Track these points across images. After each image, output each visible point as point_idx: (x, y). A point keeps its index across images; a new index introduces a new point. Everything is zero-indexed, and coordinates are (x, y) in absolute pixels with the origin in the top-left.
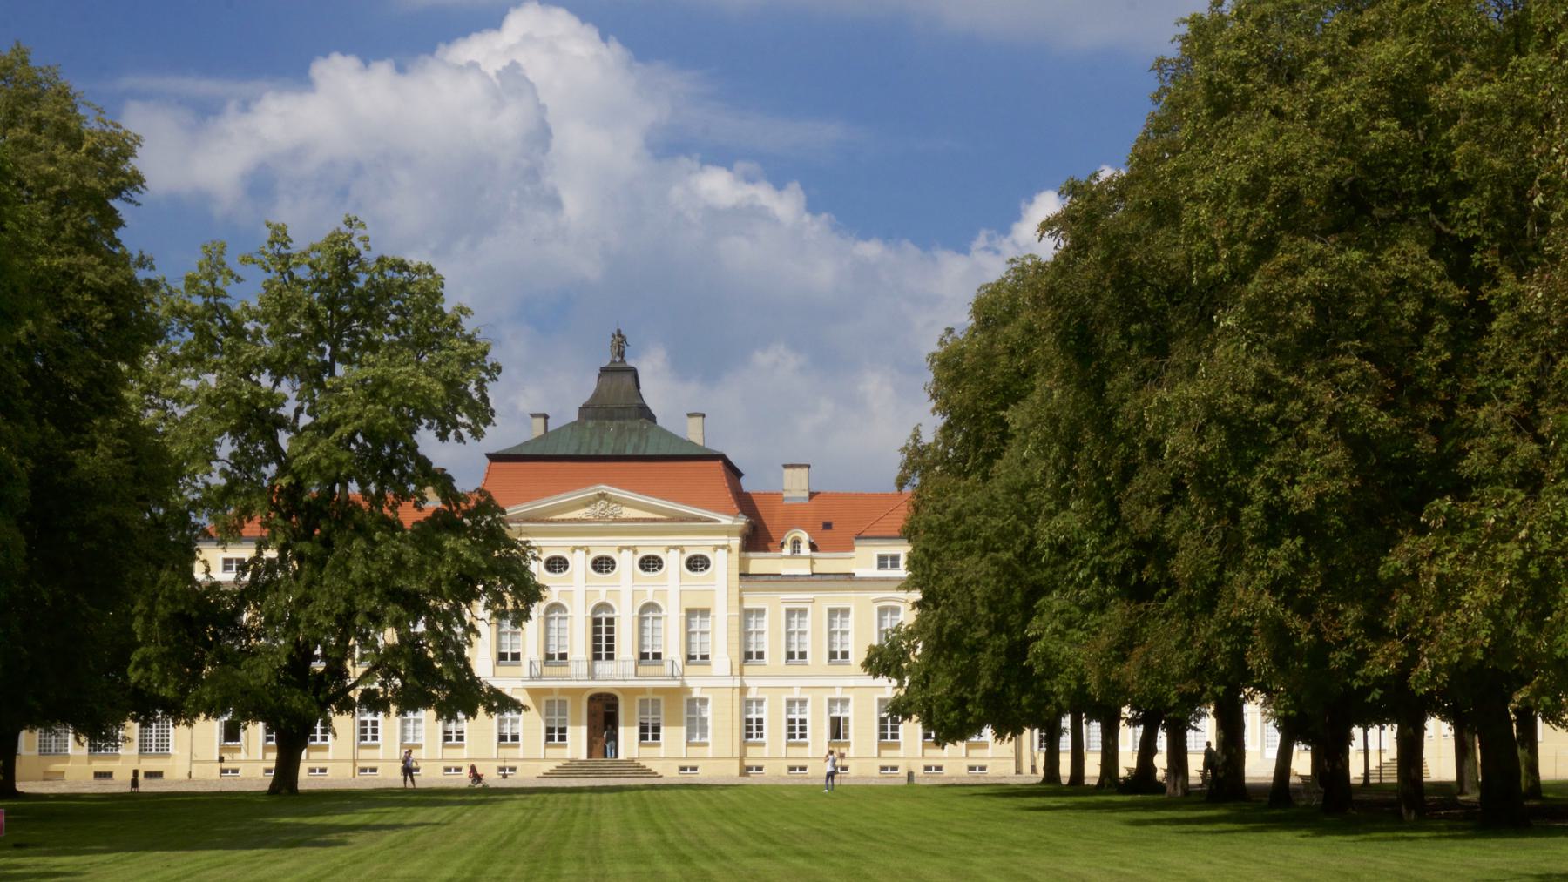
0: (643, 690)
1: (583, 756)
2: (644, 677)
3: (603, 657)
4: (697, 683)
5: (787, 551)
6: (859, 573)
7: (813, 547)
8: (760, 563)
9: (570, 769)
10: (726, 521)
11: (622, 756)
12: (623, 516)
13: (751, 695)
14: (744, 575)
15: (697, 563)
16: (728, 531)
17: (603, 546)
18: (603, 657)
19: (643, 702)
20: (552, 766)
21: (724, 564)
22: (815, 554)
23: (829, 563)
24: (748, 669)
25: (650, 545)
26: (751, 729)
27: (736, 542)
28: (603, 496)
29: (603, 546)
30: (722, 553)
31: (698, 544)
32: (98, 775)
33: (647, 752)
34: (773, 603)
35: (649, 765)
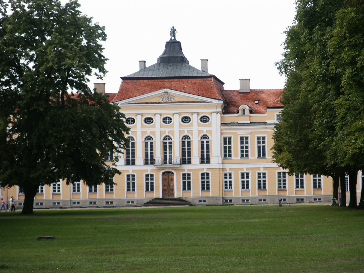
3: (228, 175)
6: (269, 122)
7: (251, 112)
8: (230, 118)
9: (155, 202)
10: (215, 102)
11: (176, 196)
12: (175, 101)
13: (228, 172)
14: (223, 124)
15: (204, 119)
16: (217, 106)
17: (167, 112)
18: (228, 175)
20: (148, 201)
21: (216, 119)
22: (251, 115)
23: (257, 117)
24: (226, 161)
25: (186, 111)
26: (228, 185)
27: (220, 110)
28: (167, 92)
29: (167, 112)
31: (204, 111)
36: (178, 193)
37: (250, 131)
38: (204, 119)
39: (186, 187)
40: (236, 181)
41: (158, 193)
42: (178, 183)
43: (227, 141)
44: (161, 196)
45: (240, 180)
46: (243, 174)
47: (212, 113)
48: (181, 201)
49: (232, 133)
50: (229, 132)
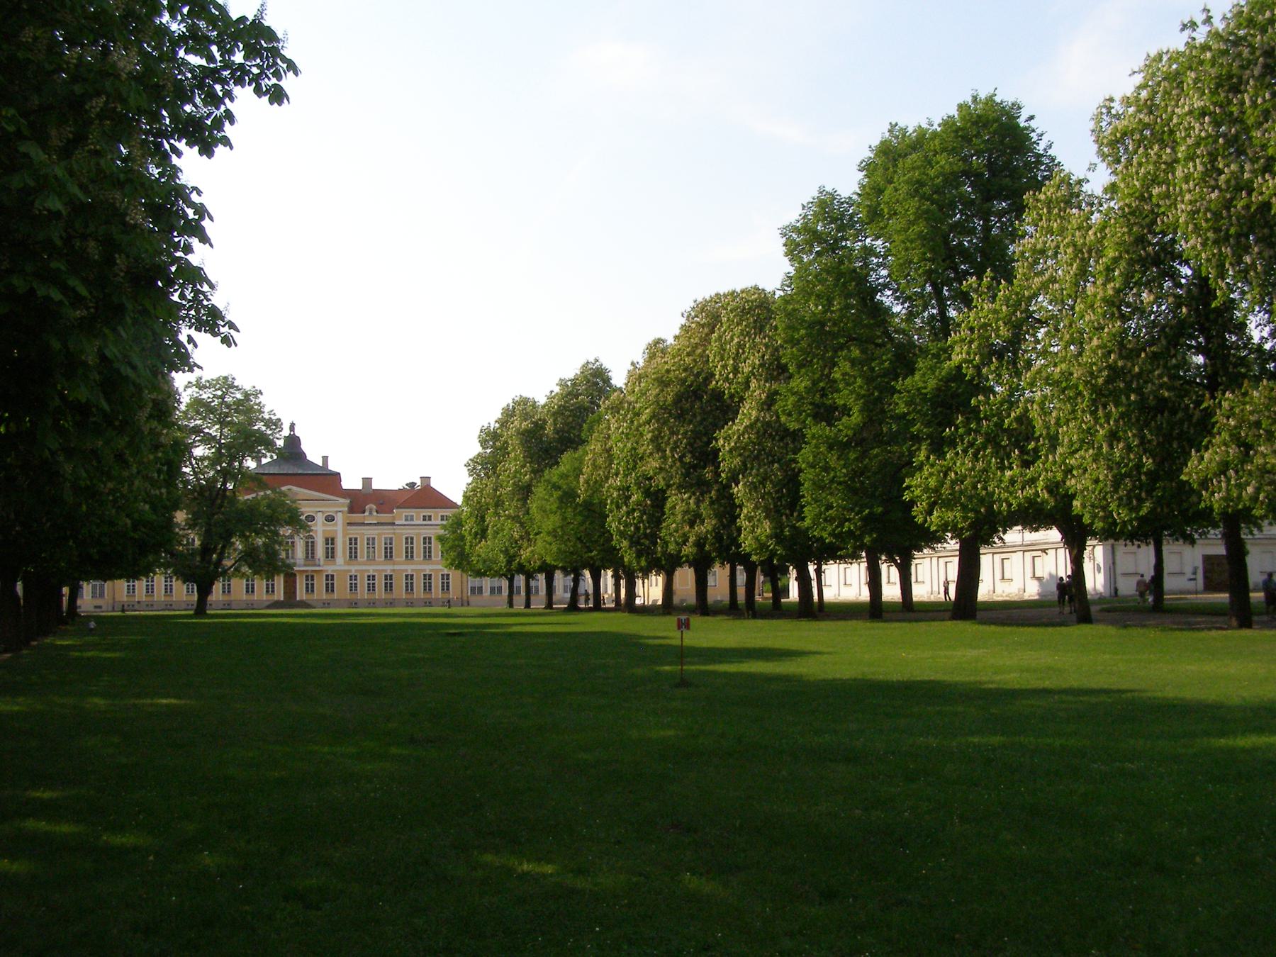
0: (307, 571)
1: (282, 599)
2: (309, 565)
4: (329, 569)
5: (367, 514)
7: (377, 512)
8: (357, 517)
9: (277, 604)
11: (298, 599)
15: (330, 519)
16: (342, 505)
19: (307, 576)
21: (339, 518)
23: (385, 517)
30: (340, 514)
31: (330, 510)
32: (96, 607)
33: (310, 597)
34: (363, 533)
35: (310, 602)
36: (301, 594)
37: (376, 532)
38: (330, 519)
39: (310, 589)
40: (363, 584)
41: (279, 594)
42: (301, 584)
43: (353, 541)
44: (282, 599)
45: (366, 582)
46: (369, 576)
47: (337, 512)
48: (304, 604)
49: (357, 534)
50: (355, 532)
